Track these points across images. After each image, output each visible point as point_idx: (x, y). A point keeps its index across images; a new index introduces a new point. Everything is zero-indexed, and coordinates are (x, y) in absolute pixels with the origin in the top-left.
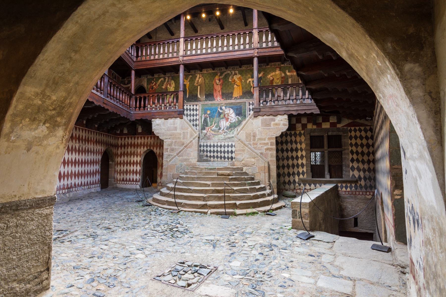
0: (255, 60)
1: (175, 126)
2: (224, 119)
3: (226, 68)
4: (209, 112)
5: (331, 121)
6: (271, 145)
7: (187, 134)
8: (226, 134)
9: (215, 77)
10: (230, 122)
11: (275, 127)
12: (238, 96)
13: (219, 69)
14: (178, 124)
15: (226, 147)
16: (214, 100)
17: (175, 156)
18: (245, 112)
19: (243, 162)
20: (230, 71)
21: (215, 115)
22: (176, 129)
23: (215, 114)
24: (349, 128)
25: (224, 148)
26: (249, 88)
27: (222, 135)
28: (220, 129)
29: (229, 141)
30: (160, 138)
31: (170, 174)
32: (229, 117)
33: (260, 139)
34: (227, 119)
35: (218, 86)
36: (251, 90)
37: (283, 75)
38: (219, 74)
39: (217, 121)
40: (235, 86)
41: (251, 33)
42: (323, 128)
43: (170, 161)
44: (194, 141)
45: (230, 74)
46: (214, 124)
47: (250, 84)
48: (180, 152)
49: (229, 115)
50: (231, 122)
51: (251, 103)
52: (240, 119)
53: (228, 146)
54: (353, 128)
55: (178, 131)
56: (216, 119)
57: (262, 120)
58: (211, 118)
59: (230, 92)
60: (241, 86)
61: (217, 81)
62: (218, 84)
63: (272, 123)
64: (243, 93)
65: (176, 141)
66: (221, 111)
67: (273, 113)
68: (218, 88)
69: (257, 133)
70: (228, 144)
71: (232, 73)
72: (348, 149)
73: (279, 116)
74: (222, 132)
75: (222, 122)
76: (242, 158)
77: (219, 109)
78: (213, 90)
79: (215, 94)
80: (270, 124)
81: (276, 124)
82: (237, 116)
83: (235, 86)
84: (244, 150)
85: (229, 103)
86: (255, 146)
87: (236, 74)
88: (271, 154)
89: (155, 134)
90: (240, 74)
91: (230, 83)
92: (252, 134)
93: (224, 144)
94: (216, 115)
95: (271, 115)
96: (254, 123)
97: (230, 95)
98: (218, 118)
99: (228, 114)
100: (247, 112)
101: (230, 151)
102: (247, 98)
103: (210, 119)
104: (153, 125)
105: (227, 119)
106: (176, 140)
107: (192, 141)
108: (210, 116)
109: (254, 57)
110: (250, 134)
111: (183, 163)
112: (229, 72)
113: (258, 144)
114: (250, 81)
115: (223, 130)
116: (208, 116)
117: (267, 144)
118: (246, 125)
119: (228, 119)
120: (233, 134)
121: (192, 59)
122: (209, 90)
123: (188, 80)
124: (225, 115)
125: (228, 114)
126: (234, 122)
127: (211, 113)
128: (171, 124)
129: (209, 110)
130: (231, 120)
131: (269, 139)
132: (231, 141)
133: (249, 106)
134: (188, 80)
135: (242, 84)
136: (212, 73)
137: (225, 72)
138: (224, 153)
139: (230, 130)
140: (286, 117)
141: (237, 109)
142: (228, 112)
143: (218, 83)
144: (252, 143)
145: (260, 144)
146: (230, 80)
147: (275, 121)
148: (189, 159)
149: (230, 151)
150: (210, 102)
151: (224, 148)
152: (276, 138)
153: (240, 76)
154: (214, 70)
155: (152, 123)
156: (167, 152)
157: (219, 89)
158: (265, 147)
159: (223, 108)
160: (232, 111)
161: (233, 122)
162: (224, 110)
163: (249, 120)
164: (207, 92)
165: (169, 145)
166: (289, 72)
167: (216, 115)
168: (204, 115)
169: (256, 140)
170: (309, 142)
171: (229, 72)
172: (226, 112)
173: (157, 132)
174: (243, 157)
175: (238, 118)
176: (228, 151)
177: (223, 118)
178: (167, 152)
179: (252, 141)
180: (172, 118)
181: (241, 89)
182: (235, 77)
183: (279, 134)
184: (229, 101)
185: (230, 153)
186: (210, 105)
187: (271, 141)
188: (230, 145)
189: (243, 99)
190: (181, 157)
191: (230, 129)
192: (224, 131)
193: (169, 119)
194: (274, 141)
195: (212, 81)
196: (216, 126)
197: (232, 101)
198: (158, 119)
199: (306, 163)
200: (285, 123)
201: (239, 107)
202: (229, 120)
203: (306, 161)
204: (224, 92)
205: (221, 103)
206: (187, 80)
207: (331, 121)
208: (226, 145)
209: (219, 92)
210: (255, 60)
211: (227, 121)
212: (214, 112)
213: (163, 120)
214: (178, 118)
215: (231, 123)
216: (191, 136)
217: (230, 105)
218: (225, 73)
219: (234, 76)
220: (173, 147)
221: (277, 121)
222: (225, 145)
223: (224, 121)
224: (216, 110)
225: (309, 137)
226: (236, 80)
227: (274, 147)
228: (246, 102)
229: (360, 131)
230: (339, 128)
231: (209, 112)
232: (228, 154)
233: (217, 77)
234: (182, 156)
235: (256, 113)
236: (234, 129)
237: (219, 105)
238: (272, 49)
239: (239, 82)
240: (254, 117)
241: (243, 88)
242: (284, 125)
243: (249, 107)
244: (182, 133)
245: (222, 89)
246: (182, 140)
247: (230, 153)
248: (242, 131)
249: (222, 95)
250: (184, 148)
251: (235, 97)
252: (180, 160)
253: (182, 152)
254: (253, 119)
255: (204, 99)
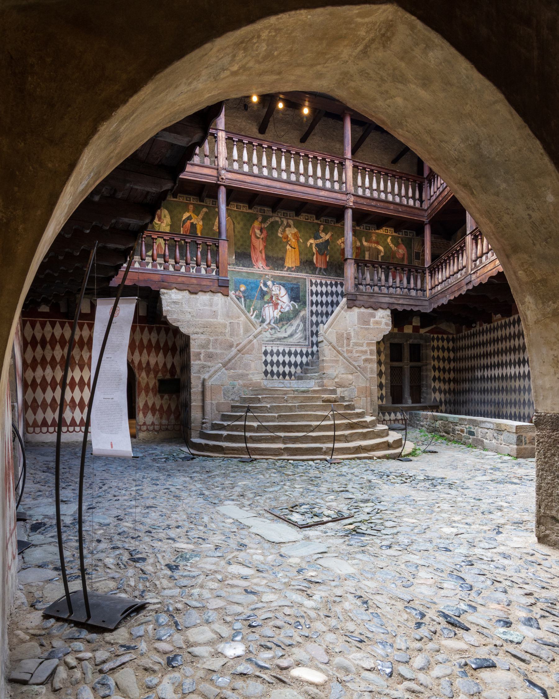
0: (349, 214)
1: (214, 309)
2: (271, 304)
3: (274, 211)
4: (243, 288)
5: (414, 324)
6: (371, 354)
7: (239, 327)
8: (273, 331)
9: (253, 222)
10: (280, 311)
11: (376, 327)
12: (294, 266)
13: (261, 209)
14: (220, 305)
15: (275, 355)
16: (252, 266)
17: (220, 369)
18: (305, 296)
19: (336, 380)
20: (280, 218)
21: (254, 295)
22: (215, 314)
23: (254, 292)
24: (432, 335)
25: (272, 356)
26: (309, 256)
27: (268, 333)
28: (263, 321)
29: (280, 344)
30: (184, 330)
31: (212, 403)
32: (279, 301)
33: (356, 344)
34: (276, 305)
35: (258, 240)
36: (313, 259)
37: (358, 244)
38: (260, 219)
39: (259, 306)
40: (288, 247)
41: (342, 165)
42: (405, 333)
43: (210, 377)
44: (255, 340)
45: (280, 223)
46: (254, 312)
47: (312, 249)
48: (230, 360)
49: (280, 298)
50: (282, 310)
51: (314, 281)
52: (297, 307)
53: (278, 354)
54: (436, 336)
55: (220, 320)
56: (256, 303)
57: (359, 314)
58: (248, 300)
59: (280, 256)
60: (297, 250)
61: (258, 232)
62: (258, 238)
63: (372, 320)
64: (301, 262)
65: (216, 340)
66: (265, 289)
67: (374, 306)
68: (259, 244)
69: (352, 334)
70: (278, 350)
71: (282, 222)
72: (431, 363)
73: (380, 310)
74: (267, 328)
75: (267, 309)
76: (335, 374)
77: (262, 285)
78: (250, 247)
79: (253, 255)
80: (370, 321)
81: (377, 323)
82: (292, 302)
83: (288, 247)
84: (338, 360)
85: (279, 276)
86: (350, 354)
87: (290, 226)
88: (370, 368)
89: (170, 321)
90: (297, 228)
91: (279, 240)
92: (345, 335)
93: (271, 348)
94: (256, 294)
95: (371, 307)
96: (347, 316)
97: (280, 262)
98: (259, 301)
99: (277, 296)
100: (308, 298)
101: (281, 361)
102: (307, 273)
103: (245, 300)
104: (164, 303)
105: (276, 305)
106: (216, 337)
107: (251, 341)
108: (245, 295)
109: (347, 208)
110: (343, 334)
111: (236, 383)
112: (277, 219)
113: (354, 351)
114: (311, 244)
115: (269, 323)
116: (241, 295)
117: (365, 352)
118: (337, 319)
119: (278, 304)
120: (286, 332)
121: (244, 180)
122: (242, 245)
123: (201, 216)
124: (272, 297)
125: (277, 296)
126: (288, 311)
127: (247, 289)
128: (205, 305)
129: (244, 284)
130: (282, 307)
131: (369, 344)
132: (282, 344)
133: (311, 286)
134: (201, 216)
135: (299, 246)
136: (248, 213)
137: (272, 217)
138: (272, 366)
139: (280, 325)
140: (388, 312)
141: (292, 289)
142: (278, 292)
143: (259, 236)
144: (345, 350)
145: (357, 352)
146: (280, 235)
147: (375, 318)
148: (248, 375)
149: (281, 361)
150: (245, 269)
151: (272, 356)
152: (378, 343)
153: (296, 230)
154: (250, 208)
155: (162, 297)
156: (200, 359)
157: (261, 247)
158: (363, 357)
159: (269, 283)
160: (283, 291)
161: (286, 310)
162: (271, 287)
163: (340, 312)
164: (238, 248)
165: (205, 346)
166: (366, 241)
167: (256, 294)
168: (233, 292)
169: (351, 346)
170: (388, 352)
171: (277, 219)
172: (273, 293)
173: (175, 317)
174: (337, 372)
175: (292, 304)
176: (278, 361)
177: (268, 303)
178: (200, 359)
179: (345, 346)
180: (205, 292)
181: (298, 255)
182: (288, 230)
183: (380, 338)
184: (278, 273)
185: (281, 366)
186: (244, 274)
187: (370, 348)
188: (281, 351)
189: (301, 272)
190: (232, 371)
191: (281, 323)
192: (270, 326)
193: (200, 293)
194: (374, 348)
195: (249, 230)
196: (256, 315)
197: (284, 273)
198: (174, 290)
199: (386, 383)
200: (388, 321)
201: (295, 286)
202: (279, 307)
203: (386, 379)
204: (270, 254)
205: (266, 275)
206: (198, 216)
207: (414, 324)
208: (275, 351)
209: (261, 252)
210: (349, 214)
211: (275, 309)
212: (252, 289)
213: (186, 293)
214: (220, 294)
215: (282, 312)
216: (247, 331)
217: (280, 280)
218: (272, 220)
219: (287, 229)
220: (211, 350)
221: (377, 318)
222: (272, 351)
223: (271, 308)
224: (257, 286)
225: (389, 345)
226: (289, 236)
227: (375, 357)
228: (305, 279)
229: (443, 340)
230: (422, 334)
231: (243, 288)
232: (278, 367)
233: (256, 224)
234: (235, 369)
235: (351, 302)
236: (287, 324)
237: (262, 277)
238: (371, 201)
239: (294, 240)
240: (348, 307)
241: (300, 254)
242: (387, 324)
243: (310, 288)
244: (228, 324)
245: (265, 247)
246: (228, 337)
247: (281, 366)
248: (330, 329)
249: (266, 259)
250: (236, 355)
251: (289, 268)
252: (230, 377)
253: (233, 361)
254: (346, 311)
255: (234, 262)
